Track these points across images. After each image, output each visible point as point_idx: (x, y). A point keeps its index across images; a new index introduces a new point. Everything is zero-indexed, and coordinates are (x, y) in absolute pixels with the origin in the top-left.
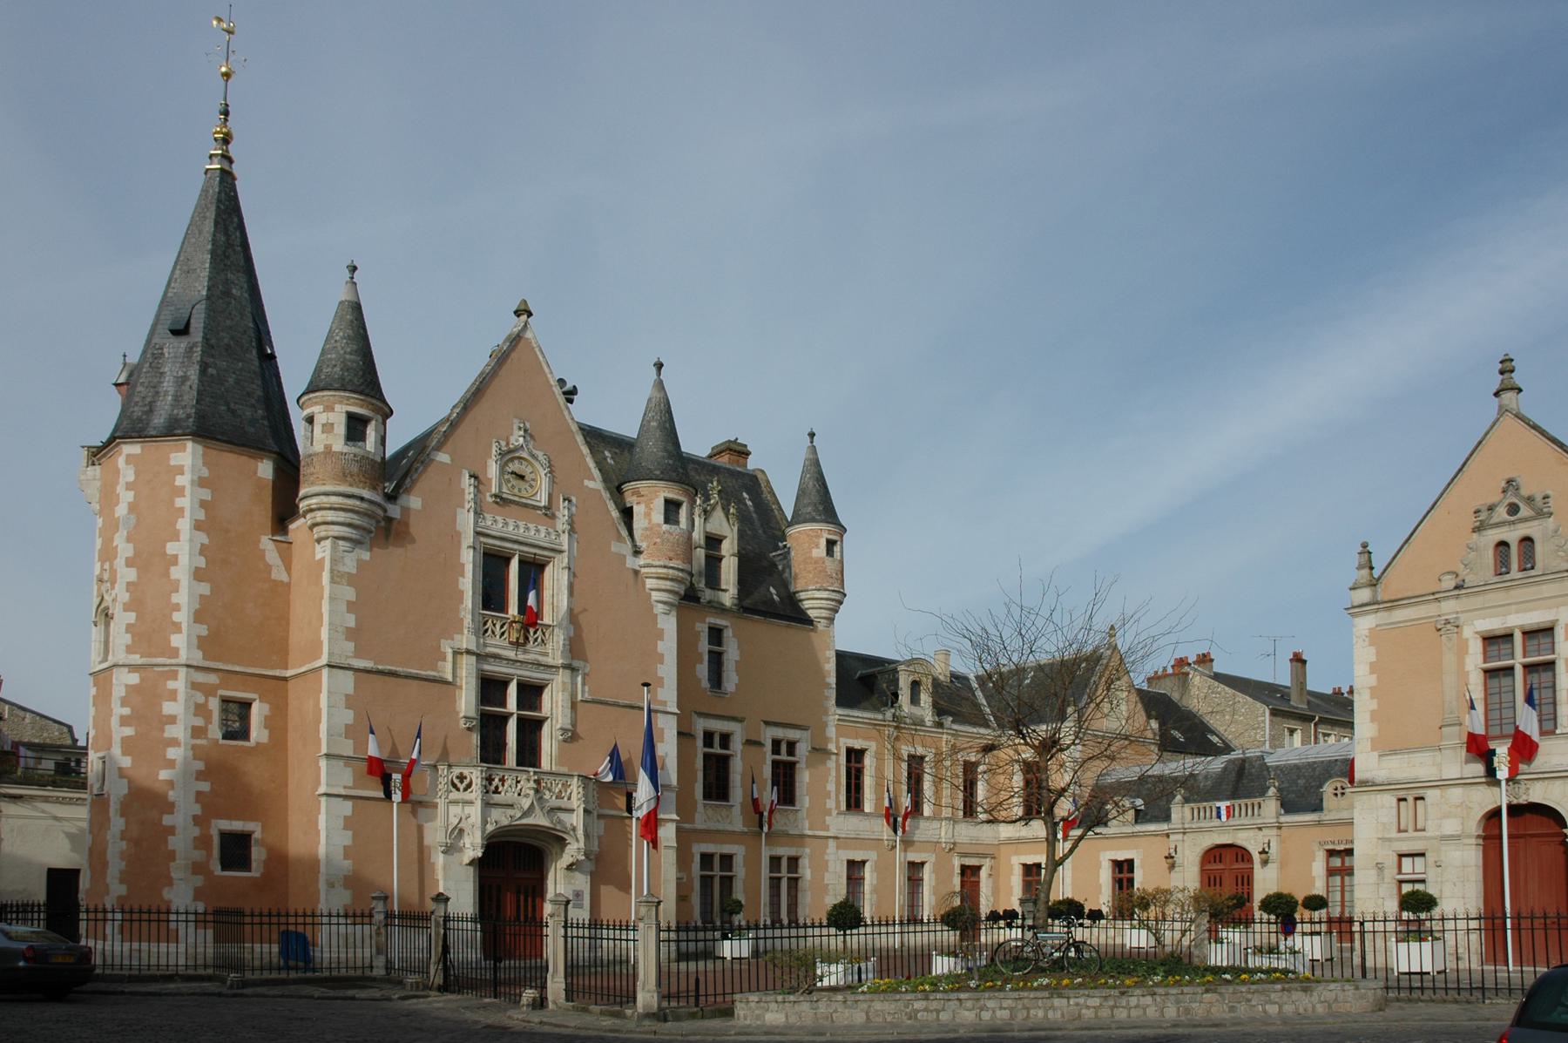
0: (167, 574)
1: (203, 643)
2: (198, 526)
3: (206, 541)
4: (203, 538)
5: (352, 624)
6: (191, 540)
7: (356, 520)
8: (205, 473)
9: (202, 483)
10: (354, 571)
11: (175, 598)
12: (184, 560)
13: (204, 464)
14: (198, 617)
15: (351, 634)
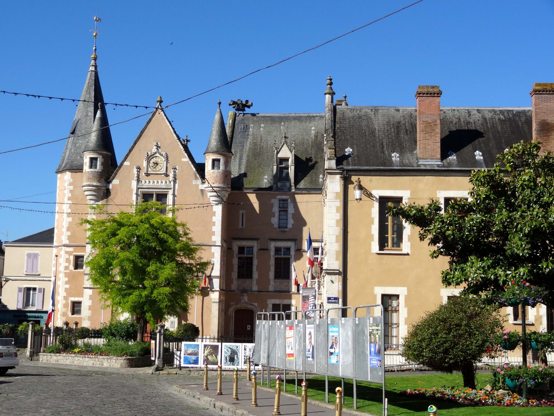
1: (69, 238)
7: (94, 193)
8: (72, 181)
9: (70, 184)
14: (68, 229)
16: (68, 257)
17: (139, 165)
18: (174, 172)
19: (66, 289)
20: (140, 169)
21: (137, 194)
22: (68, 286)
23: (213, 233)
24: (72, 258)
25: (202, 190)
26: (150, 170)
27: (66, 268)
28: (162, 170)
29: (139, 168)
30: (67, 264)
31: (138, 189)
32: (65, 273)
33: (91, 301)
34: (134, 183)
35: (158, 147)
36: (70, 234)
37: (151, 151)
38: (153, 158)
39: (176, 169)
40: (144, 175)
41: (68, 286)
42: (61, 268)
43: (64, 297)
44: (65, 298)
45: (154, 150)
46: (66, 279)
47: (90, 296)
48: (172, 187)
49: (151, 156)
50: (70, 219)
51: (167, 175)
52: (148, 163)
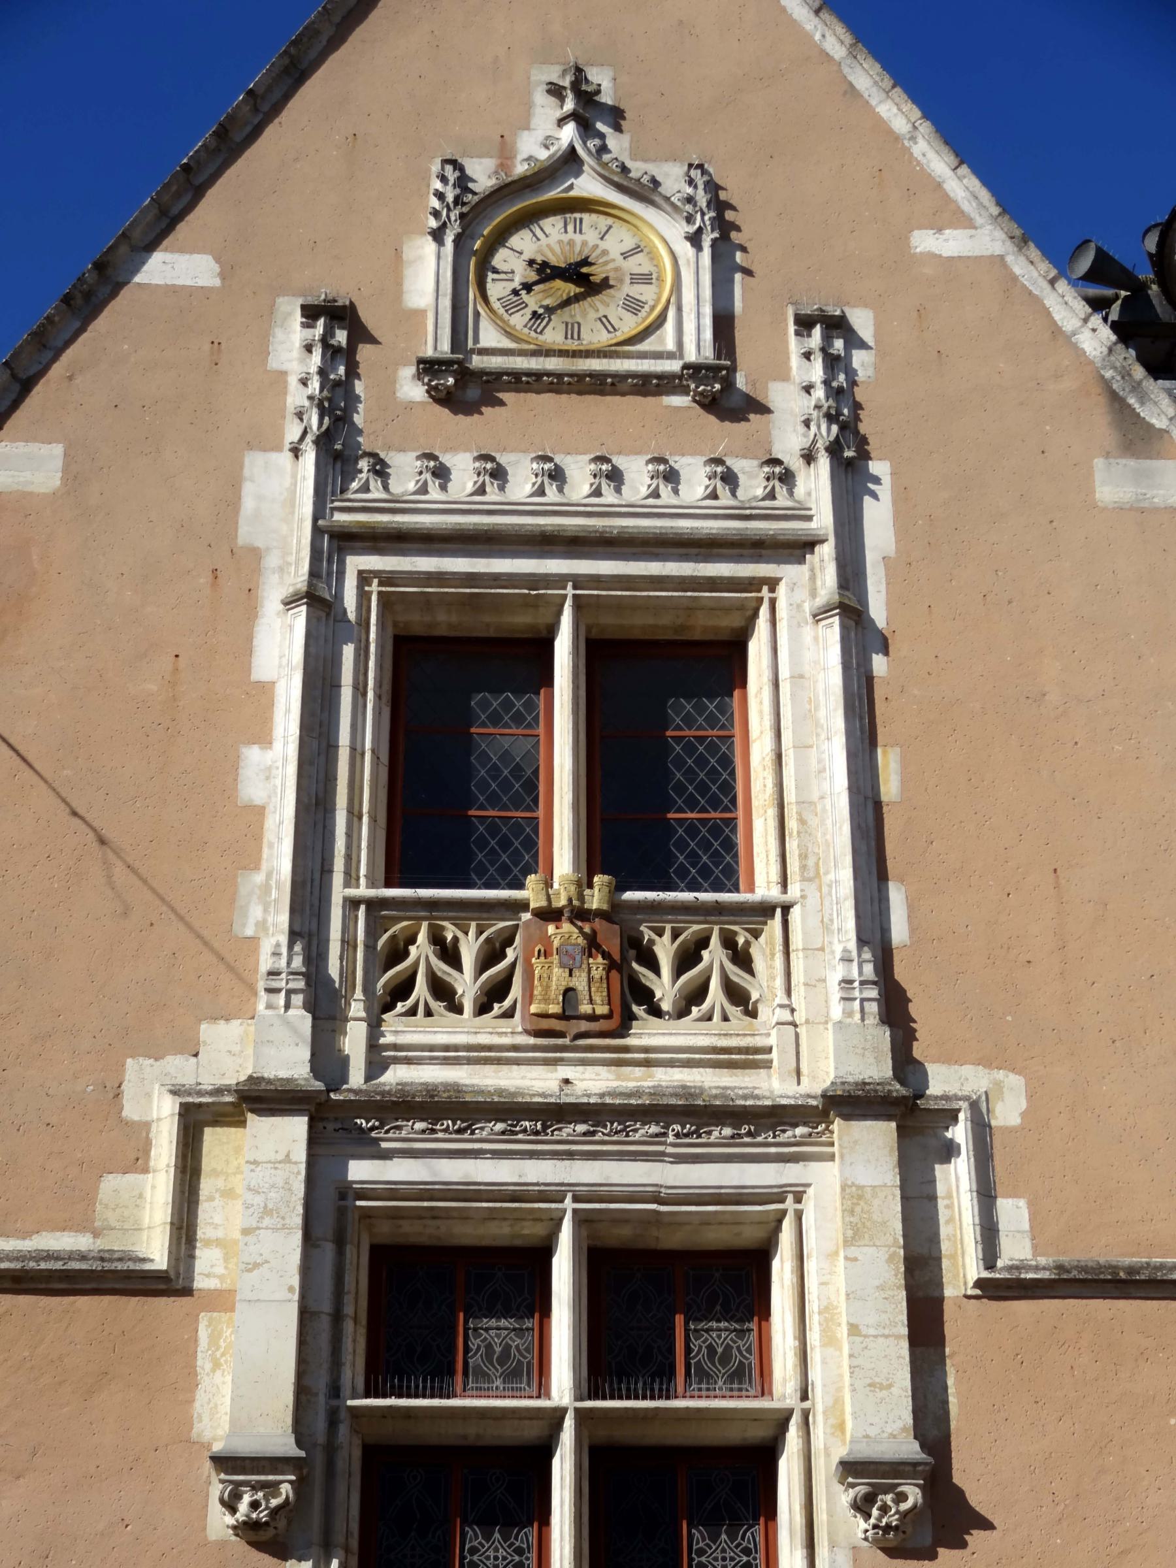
17: (342, 290)
18: (833, 363)
20: (360, 334)
21: (318, 601)
26: (490, 336)
28: (667, 338)
29: (341, 325)
31: (334, 542)
34: (280, 494)
35: (588, 109)
37: (505, 152)
38: (528, 218)
39: (837, 325)
40: (413, 390)
45: (546, 132)
48: (823, 519)
49: (505, 191)
51: (722, 393)
52: (473, 264)
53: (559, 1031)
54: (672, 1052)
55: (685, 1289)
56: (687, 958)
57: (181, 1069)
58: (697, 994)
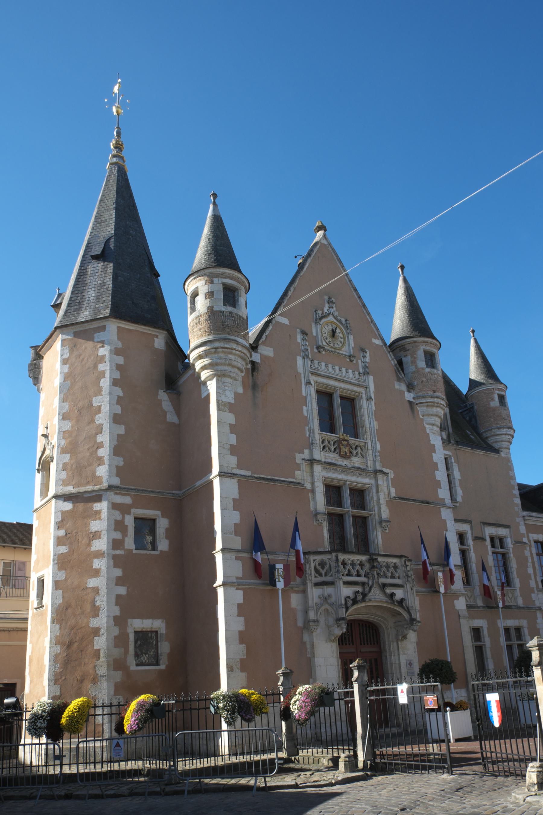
0: (93, 421)
1: (119, 471)
2: (115, 383)
3: (121, 394)
4: (119, 392)
5: (234, 442)
6: (110, 394)
8: (120, 345)
10: (233, 401)
11: (99, 439)
12: (106, 409)
13: (118, 339)
14: (116, 451)
15: (233, 450)
16: (119, 518)
19: (118, 597)
22: (122, 591)
23: (438, 484)
24: (129, 521)
25: (410, 402)
27: (116, 544)
30: (118, 535)
32: (115, 557)
33: (242, 619)
36: (122, 464)
41: (122, 591)
42: (101, 545)
43: (115, 618)
44: (119, 621)
46: (118, 572)
47: (239, 605)
50: (121, 430)
53: (344, 456)
54: (356, 461)
55: (359, 495)
56: (356, 448)
57: (301, 456)
58: (357, 454)
